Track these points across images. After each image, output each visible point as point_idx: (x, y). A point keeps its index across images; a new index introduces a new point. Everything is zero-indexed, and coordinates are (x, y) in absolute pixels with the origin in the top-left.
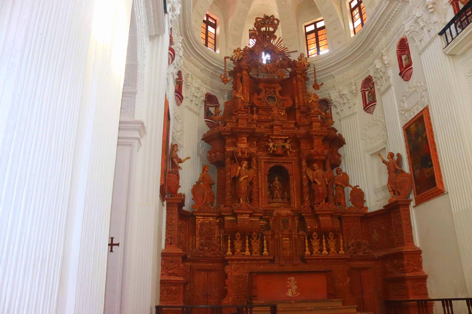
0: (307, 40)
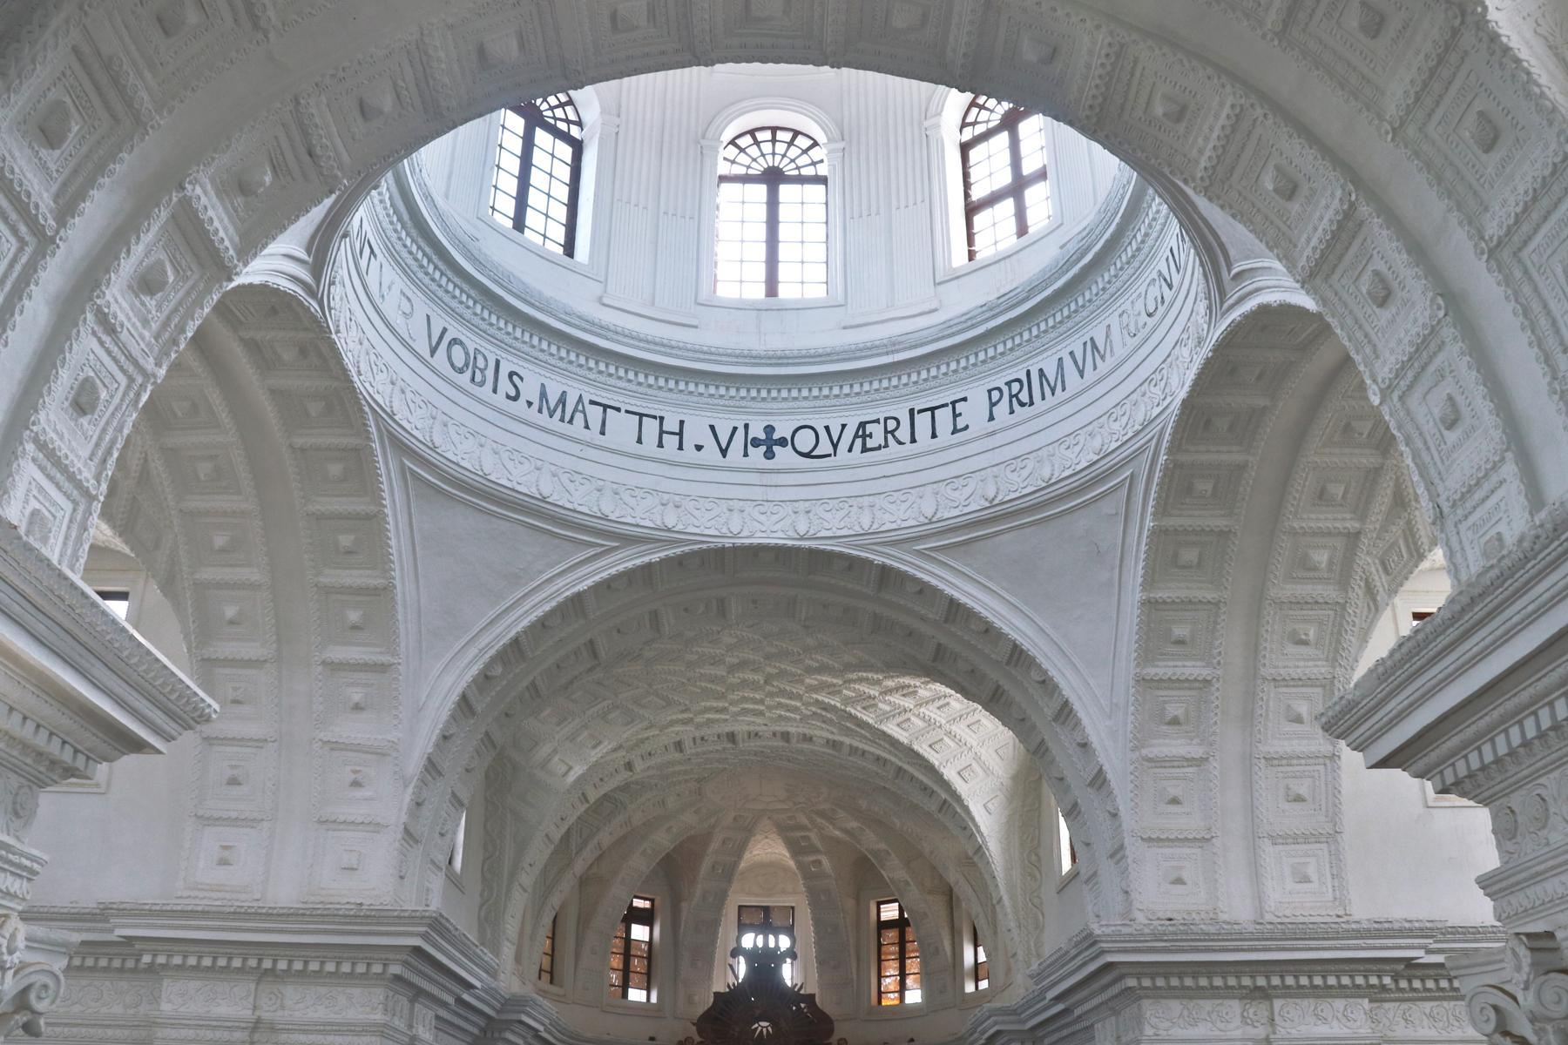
0: (880, 945)
